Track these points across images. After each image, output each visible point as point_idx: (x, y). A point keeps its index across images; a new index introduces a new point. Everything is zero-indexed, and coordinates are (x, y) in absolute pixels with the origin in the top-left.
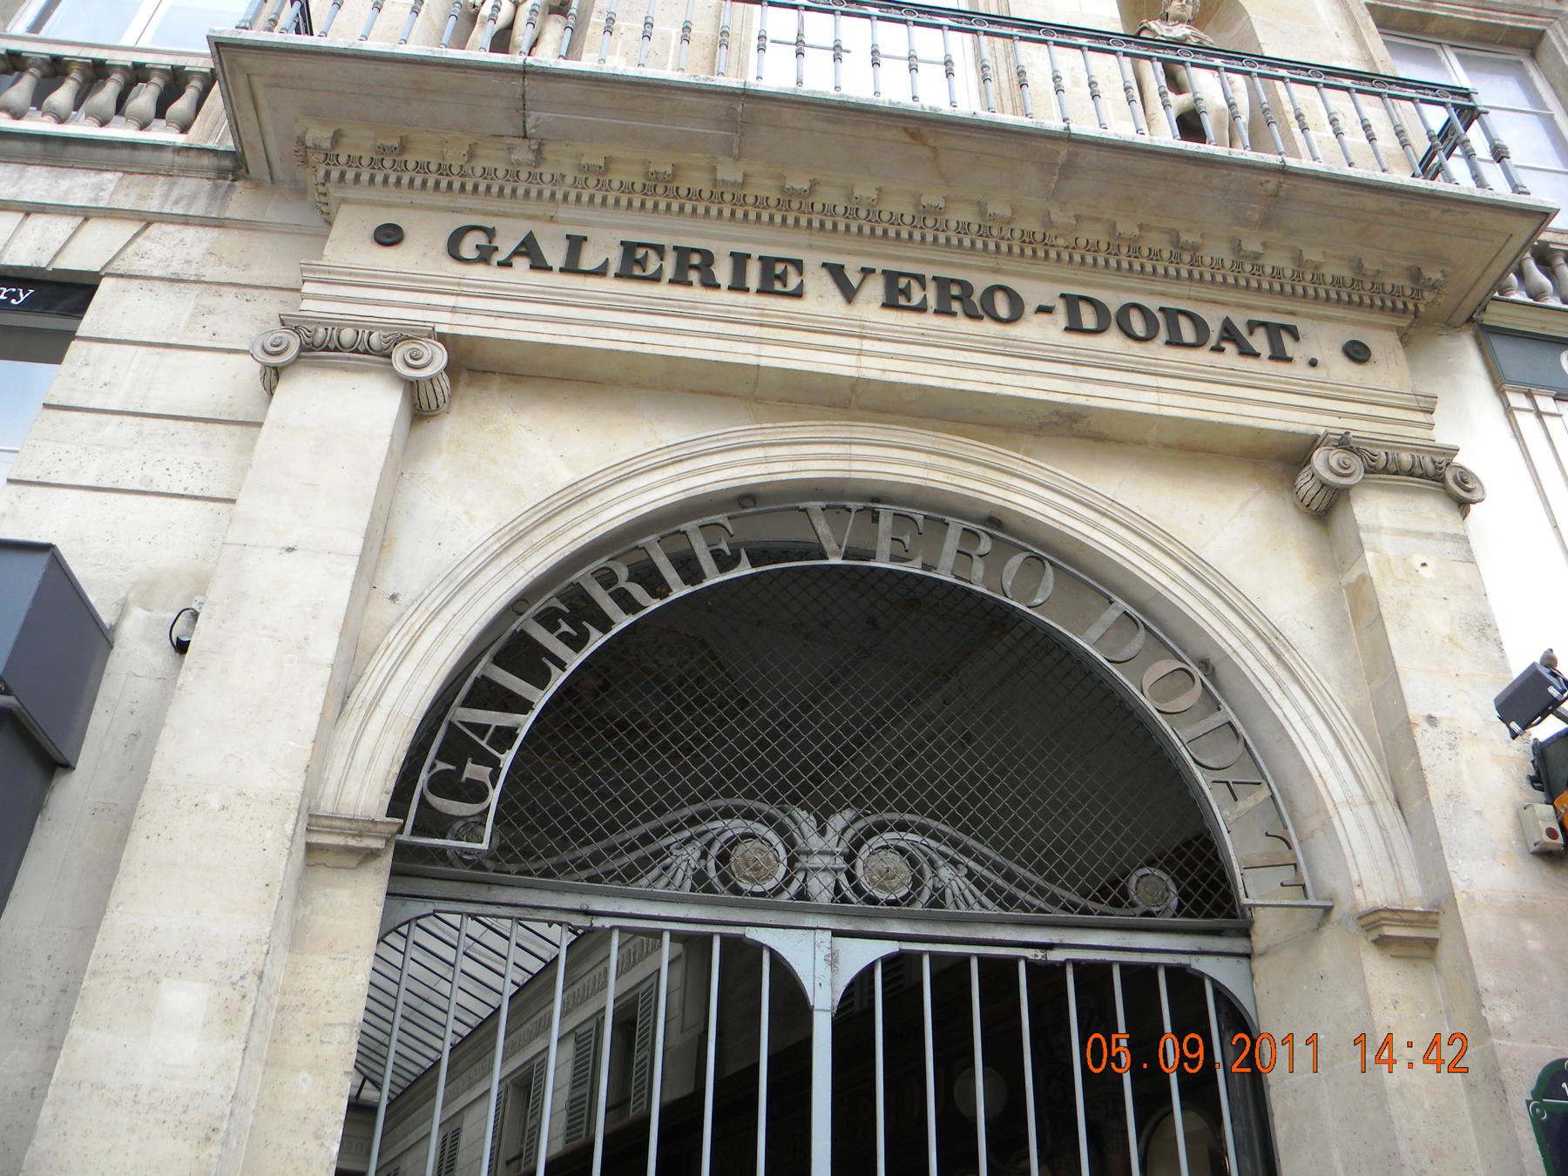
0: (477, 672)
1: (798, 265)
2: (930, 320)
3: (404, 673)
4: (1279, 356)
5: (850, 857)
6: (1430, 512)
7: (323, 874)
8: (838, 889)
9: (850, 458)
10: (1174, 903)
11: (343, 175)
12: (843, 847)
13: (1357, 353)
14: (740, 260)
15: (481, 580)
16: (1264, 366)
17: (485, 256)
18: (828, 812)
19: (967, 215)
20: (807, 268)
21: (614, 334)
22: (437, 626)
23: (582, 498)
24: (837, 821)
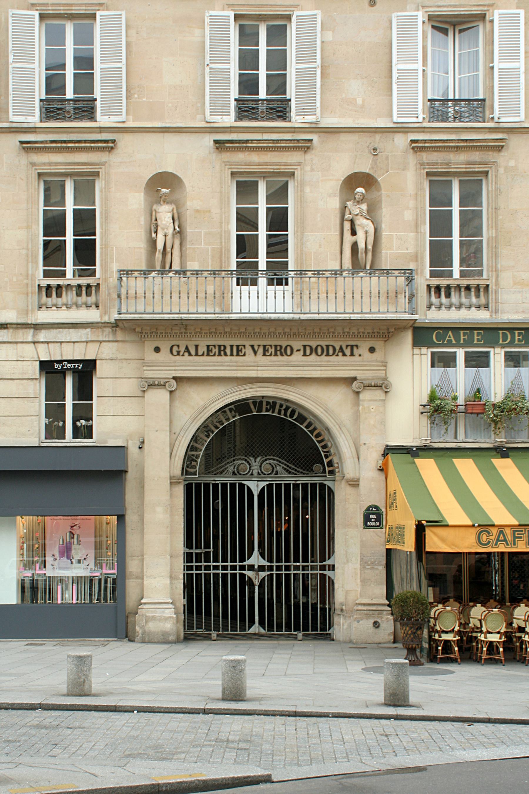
0: (191, 444)
1: (244, 346)
2: (273, 358)
3: (180, 449)
4: (352, 354)
5: (260, 466)
6: (378, 394)
7: (173, 486)
8: (258, 472)
9: (257, 391)
10: (321, 471)
11: (144, 336)
12: (259, 465)
13: (372, 350)
14: (232, 346)
15: (190, 428)
16: (348, 359)
17: (178, 353)
18: (256, 458)
19: (281, 331)
20: (246, 347)
21: (208, 372)
22: (184, 439)
23: (206, 408)
24: (258, 460)
